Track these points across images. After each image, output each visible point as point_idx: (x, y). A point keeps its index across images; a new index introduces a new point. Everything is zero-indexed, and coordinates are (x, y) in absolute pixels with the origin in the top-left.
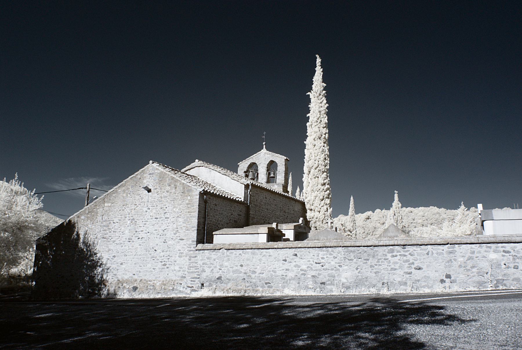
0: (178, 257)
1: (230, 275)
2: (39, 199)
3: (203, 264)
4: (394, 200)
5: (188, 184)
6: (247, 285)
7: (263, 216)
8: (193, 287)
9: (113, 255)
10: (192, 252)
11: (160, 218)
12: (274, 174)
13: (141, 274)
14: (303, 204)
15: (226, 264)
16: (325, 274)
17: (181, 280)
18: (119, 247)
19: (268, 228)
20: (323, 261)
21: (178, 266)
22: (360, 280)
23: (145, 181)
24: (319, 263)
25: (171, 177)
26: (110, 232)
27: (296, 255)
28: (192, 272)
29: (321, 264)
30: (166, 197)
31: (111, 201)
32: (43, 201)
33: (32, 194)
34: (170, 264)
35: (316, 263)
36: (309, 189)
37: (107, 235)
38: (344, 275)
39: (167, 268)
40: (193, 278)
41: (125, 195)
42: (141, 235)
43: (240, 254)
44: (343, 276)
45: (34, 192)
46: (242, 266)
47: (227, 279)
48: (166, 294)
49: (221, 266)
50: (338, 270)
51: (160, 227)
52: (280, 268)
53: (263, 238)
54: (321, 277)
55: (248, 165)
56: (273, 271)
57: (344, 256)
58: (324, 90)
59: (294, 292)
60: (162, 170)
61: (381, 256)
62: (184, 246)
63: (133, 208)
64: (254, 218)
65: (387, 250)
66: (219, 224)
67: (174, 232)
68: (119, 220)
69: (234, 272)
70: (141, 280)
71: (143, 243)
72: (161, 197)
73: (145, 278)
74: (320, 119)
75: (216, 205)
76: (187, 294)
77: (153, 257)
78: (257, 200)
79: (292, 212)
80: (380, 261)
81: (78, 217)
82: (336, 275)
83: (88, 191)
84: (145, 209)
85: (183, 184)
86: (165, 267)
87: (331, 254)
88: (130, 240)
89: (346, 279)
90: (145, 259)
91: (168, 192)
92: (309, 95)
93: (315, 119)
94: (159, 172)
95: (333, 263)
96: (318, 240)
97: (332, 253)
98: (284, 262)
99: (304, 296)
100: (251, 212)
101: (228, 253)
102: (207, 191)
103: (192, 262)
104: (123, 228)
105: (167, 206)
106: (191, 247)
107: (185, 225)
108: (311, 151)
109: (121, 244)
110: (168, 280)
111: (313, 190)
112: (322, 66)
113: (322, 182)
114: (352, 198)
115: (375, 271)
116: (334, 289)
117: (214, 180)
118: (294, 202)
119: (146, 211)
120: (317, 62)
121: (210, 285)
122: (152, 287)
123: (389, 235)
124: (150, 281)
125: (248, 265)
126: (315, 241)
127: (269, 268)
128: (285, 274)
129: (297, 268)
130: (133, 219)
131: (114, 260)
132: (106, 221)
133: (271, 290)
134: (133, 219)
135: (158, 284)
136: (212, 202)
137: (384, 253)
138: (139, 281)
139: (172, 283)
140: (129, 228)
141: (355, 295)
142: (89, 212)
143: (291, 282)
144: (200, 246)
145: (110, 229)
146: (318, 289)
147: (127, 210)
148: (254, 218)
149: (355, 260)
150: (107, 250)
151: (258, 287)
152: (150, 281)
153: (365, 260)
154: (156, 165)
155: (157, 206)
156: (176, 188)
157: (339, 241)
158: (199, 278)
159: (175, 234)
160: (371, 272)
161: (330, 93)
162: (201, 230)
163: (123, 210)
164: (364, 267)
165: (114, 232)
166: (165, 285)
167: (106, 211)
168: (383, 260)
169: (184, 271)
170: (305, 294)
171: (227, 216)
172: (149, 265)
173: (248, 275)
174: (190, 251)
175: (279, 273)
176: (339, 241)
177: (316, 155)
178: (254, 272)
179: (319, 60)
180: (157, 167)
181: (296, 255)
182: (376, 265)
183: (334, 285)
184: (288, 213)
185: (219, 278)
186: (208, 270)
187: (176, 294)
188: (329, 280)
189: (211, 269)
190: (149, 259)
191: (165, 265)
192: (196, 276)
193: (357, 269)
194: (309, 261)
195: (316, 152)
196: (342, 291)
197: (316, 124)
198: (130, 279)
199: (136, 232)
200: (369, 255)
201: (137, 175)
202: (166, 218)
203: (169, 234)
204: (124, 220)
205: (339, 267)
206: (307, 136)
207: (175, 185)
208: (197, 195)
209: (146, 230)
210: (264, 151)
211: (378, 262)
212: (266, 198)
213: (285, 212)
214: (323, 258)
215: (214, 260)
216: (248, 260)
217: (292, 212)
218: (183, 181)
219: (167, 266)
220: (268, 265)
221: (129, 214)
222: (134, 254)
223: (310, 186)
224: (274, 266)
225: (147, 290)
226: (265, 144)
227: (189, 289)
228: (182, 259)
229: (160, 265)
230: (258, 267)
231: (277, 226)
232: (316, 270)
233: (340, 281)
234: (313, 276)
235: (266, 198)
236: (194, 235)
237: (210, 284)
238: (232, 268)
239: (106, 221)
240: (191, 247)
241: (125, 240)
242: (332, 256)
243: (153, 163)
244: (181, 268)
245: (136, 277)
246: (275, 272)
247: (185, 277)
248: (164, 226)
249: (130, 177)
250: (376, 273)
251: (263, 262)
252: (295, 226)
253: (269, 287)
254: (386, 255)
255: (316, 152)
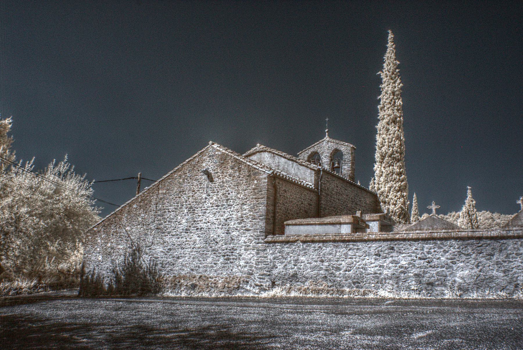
0: (243, 251)
1: (308, 272)
2: (90, 183)
3: (274, 258)
4: (467, 197)
5: (255, 166)
6: (330, 284)
7: (334, 208)
8: (262, 285)
9: (169, 247)
10: (260, 245)
11: (222, 205)
12: (339, 164)
13: (201, 270)
14: (374, 195)
15: (302, 258)
16: (432, 272)
17: (248, 278)
18: (174, 239)
19: (353, 217)
20: (430, 255)
21: (244, 261)
22: (483, 280)
23: (204, 165)
24: (424, 259)
25: (234, 158)
26: (165, 222)
27: (392, 248)
28: (261, 268)
29: (427, 260)
30: (229, 181)
31: (166, 188)
32: (93, 187)
33: (82, 179)
34: (233, 259)
35: (420, 259)
36: (382, 179)
37: (162, 226)
38: (459, 274)
39: (231, 263)
40: (262, 275)
41: (181, 180)
42: (201, 225)
43: (320, 247)
44: (458, 275)
45: (84, 177)
46: (322, 261)
47: (304, 277)
48: (230, 293)
49: (296, 261)
50: (451, 267)
51: (222, 216)
52: (372, 265)
53: (346, 230)
54: (427, 275)
55: (307, 155)
56: (362, 268)
57: (458, 250)
58: (397, 68)
59: (391, 294)
60: (224, 151)
61: (510, 250)
62: (251, 238)
63: (191, 194)
64: (325, 208)
65: (519, 243)
66: (289, 213)
67: (239, 221)
68: (175, 209)
69: (313, 268)
70: (201, 277)
71: (202, 234)
72: (223, 182)
73: (206, 274)
74: (393, 101)
75: (285, 192)
76: (254, 293)
77: (213, 250)
78: (328, 189)
79: (364, 205)
80: (511, 256)
81: (130, 206)
82: (448, 273)
83: (139, 182)
84: (204, 196)
85: (249, 165)
86: (229, 262)
87: (440, 248)
88: (187, 231)
89: (462, 278)
90: (205, 252)
91: (230, 175)
92: (380, 75)
93: (388, 101)
94: (219, 153)
95: (443, 259)
96: (420, 230)
97: (442, 246)
98: (378, 257)
99: (406, 299)
100: (322, 202)
101: (304, 246)
102: (276, 174)
103: (261, 257)
104: (179, 218)
105: (230, 192)
106: (259, 239)
107: (251, 213)
108: (384, 136)
109: (177, 235)
110: (232, 276)
111: (385, 180)
112: (394, 41)
113: (398, 170)
114: (415, 195)
115: (503, 269)
116: (446, 292)
117: (278, 166)
118: (366, 194)
119: (206, 198)
120: (389, 37)
121: (283, 284)
122: (213, 285)
123: (520, 224)
124: (210, 278)
125: (330, 260)
126: (417, 232)
127: (358, 264)
128: (379, 272)
129: (394, 265)
130: (191, 208)
131: (169, 254)
132: (160, 210)
133: (362, 290)
134: (191, 208)
135: (220, 281)
136: (282, 187)
137: (516, 246)
138: (198, 277)
139: (237, 281)
140: (187, 217)
141: (477, 300)
142: (142, 200)
143: (387, 281)
144: (270, 238)
145: (164, 218)
146: (424, 291)
147: (184, 198)
148: (325, 208)
149: (474, 256)
150: (161, 242)
151: (343, 287)
152: (210, 278)
153: (489, 255)
154: (215, 146)
155: (218, 192)
156: (240, 171)
157: (450, 231)
158: (269, 275)
159: (239, 223)
160: (497, 271)
161: (403, 71)
162: (269, 219)
163: (179, 197)
164: (488, 265)
165: (169, 222)
166: (228, 283)
167: (161, 199)
168: (514, 255)
169: (251, 267)
170: (406, 297)
171: (297, 205)
172: (209, 260)
173: (330, 272)
174: (258, 243)
175: (371, 270)
176: (450, 231)
177: (390, 140)
178: (338, 269)
179: (391, 36)
180: (218, 148)
181: (392, 248)
182: (505, 262)
183: (445, 286)
184: (360, 205)
185: (294, 276)
186: (280, 267)
187: (242, 293)
188: (438, 280)
189: (285, 264)
190: (210, 253)
191: (228, 259)
192: (265, 272)
193: (477, 266)
194: (411, 256)
195: (390, 137)
196: (458, 293)
197: (388, 106)
198: (188, 275)
199: (195, 221)
200: (493, 249)
201: (195, 157)
202: (229, 206)
203: (232, 224)
204: (181, 208)
205: (451, 264)
206: (379, 120)
207: (239, 168)
208: (265, 178)
209: (206, 220)
210: (327, 138)
211: (507, 256)
212: (337, 187)
213: (356, 204)
214: (429, 253)
215: (288, 254)
216: (330, 254)
217: (364, 205)
218: (248, 163)
219: (232, 260)
220: (355, 261)
221: (186, 202)
222: (193, 246)
223: (384, 175)
224: (364, 262)
225: (208, 288)
226: (328, 131)
227: (258, 287)
228: (249, 252)
229: (222, 260)
230: (343, 263)
231: (361, 214)
232: (421, 268)
233: (455, 281)
234: (415, 275)
235: (337, 187)
236: (262, 224)
237: (283, 282)
238: (310, 263)
239: (160, 210)
240: (259, 239)
241: (181, 231)
242: (442, 250)
243: (213, 144)
244: (247, 263)
245: (195, 273)
246: (365, 269)
247: (252, 274)
248: (226, 215)
249: (187, 160)
250: (504, 272)
251: (349, 257)
252: (380, 216)
253: (357, 287)
254: (519, 249)
255: (390, 137)
